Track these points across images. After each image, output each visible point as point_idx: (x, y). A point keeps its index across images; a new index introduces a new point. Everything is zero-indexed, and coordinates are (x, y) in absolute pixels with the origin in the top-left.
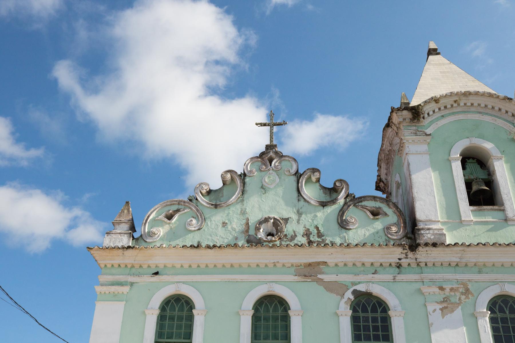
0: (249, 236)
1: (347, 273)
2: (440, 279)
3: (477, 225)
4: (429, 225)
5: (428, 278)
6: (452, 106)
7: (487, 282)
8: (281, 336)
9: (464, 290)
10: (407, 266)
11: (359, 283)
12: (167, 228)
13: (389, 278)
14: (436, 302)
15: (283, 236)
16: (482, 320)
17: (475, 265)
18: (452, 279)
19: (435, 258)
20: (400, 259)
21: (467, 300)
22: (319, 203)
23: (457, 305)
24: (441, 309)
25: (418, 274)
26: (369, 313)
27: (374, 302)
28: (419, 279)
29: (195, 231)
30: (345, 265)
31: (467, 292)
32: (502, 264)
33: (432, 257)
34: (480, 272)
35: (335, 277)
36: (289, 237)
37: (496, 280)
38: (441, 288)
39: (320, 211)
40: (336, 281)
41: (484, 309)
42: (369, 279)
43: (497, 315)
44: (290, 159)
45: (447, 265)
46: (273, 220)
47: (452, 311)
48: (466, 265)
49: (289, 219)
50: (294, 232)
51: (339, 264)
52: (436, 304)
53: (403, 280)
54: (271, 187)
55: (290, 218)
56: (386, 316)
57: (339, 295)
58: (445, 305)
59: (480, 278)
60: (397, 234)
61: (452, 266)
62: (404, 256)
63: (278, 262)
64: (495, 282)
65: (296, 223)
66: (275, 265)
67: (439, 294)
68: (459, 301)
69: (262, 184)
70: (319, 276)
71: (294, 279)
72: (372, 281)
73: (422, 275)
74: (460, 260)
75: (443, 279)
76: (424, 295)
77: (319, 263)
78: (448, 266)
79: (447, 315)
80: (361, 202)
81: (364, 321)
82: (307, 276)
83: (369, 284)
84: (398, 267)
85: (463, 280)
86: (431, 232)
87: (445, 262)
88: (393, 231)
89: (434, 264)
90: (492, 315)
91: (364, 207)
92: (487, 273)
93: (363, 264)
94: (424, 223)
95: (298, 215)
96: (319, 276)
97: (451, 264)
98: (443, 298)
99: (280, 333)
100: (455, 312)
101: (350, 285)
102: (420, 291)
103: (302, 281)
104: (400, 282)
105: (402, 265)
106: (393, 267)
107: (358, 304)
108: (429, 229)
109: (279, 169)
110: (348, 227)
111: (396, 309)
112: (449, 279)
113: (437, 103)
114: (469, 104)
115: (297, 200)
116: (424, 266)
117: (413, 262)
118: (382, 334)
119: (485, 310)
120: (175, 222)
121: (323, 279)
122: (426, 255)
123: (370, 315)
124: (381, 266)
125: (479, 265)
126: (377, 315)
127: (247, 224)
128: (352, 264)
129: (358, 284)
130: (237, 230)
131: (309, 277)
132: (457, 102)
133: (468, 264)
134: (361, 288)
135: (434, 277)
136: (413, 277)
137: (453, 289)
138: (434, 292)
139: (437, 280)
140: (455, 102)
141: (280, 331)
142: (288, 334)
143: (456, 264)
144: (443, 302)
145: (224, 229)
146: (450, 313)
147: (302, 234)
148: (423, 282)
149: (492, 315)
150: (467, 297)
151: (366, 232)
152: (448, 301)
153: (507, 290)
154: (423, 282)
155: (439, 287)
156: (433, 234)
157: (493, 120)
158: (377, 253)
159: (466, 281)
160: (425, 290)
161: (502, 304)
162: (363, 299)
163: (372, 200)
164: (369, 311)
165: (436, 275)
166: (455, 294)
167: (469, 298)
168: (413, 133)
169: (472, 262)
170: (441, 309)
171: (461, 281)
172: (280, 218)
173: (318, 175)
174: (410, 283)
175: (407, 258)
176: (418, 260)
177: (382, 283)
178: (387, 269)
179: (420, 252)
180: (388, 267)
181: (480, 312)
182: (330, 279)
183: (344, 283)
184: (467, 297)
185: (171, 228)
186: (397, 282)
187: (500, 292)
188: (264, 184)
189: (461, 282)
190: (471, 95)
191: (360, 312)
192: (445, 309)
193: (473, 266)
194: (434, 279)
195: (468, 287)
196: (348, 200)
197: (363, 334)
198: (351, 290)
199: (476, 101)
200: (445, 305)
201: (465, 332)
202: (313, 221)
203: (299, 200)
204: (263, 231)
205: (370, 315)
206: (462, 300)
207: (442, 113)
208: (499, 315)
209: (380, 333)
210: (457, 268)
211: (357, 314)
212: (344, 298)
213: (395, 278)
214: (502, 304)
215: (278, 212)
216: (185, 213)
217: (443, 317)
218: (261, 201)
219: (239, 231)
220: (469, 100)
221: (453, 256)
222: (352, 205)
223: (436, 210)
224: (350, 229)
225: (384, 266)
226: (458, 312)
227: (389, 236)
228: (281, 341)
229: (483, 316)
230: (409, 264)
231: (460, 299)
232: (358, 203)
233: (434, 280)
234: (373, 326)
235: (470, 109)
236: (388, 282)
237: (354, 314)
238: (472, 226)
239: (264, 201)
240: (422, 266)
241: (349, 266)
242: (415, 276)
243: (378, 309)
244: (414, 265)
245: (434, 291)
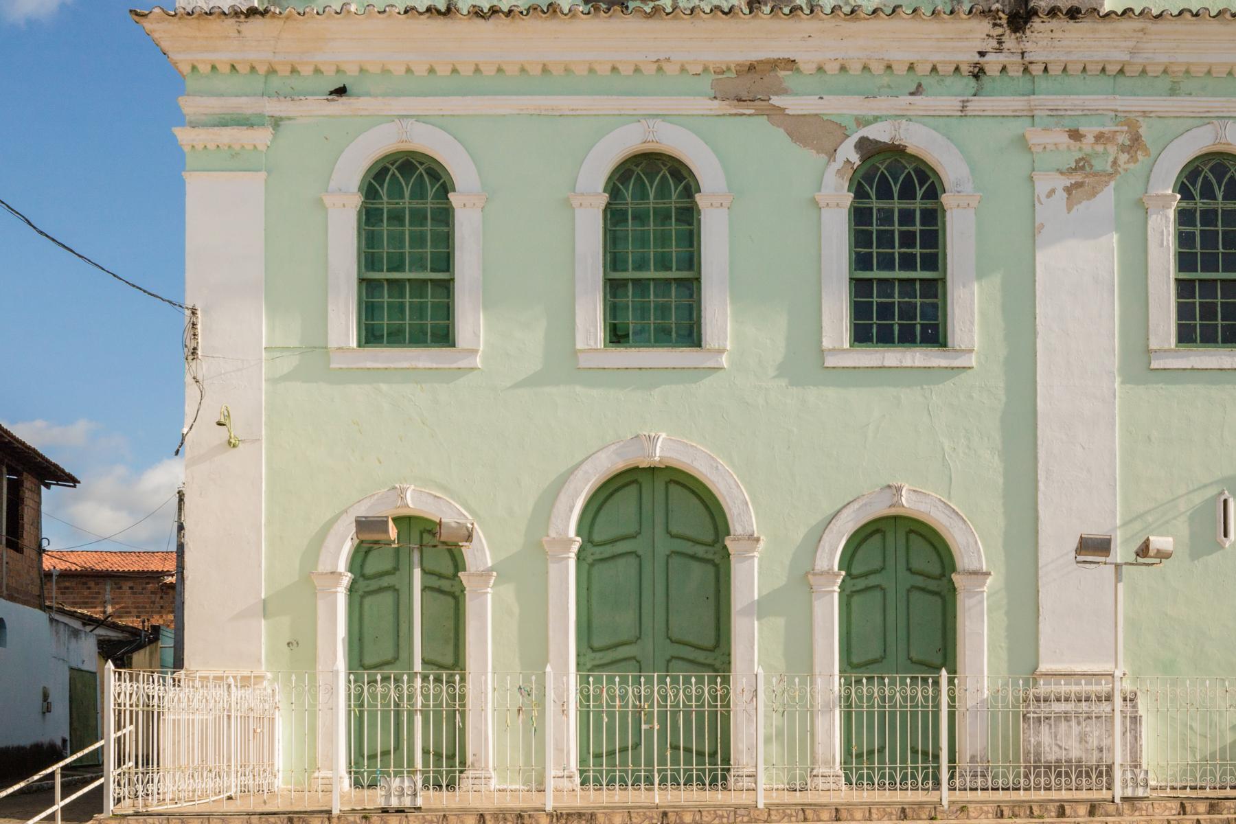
1: (846, 92)
2: (1077, 110)
5: (1046, 108)
7: (1187, 117)
8: (677, 262)
9: (1129, 140)
10: (999, 74)
11: (876, 119)
14: (1058, 170)
16: (1160, 216)
17: (1165, 72)
18: (1103, 110)
19: (1070, 52)
20: (982, 54)
21: (1131, 166)
23: (1106, 179)
24: (1068, 190)
25: (1023, 95)
26: (893, 199)
27: (909, 172)
28: (1023, 110)
30: (843, 68)
31: (1135, 143)
32: (1228, 70)
33: (1062, 47)
34: (1173, 92)
37: (1208, 112)
38: (1075, 135)
40: (817, 115)
41: (1167, 188)
42: (900, 110)
43: (1196, 204)
47: (1094, 194)
48: (1144, 72)
51: (827, 67)
52: (1058, 175)
56: (934, 206)
57: (822, 152)
58: (1078, 178)
61: (1107, 73)
62: (994, 43)
64: (1205, 119)
68: (1112, 167)
70: (776, 101)
71: (711, 110)
72: (908, 113)
73: (1032, 97)
74: (1131, 57)
75: (1083, 110)
76: (1032, 153)
77: (774, 64)
78: (1098, 73)
79: (1080, 203)
81: (881, 221)
82: (744, 99)
83: (899, 123)
84: (976, 76)
85: (1130, 112)
87: (1092, 62)
89: (1065, 69)
90: (1184, 204)
92: (1190, 94)
93: (889, 67)
96: (776, 101)
97: (1108, 67)
98: (1077, 162)
99: (674, 254)
100: (1099, 196)
101: (852, 124)
102: (1022, 142)
103: (731, 115)
104: (978, 119)
105: (987, 68)
106: (965, 76)
107: (868, 178)
111: (959, 189)
112: (1097, 110)
116: (1041, 73)
117: (1013, 63)
118: (921, 254)
119: (1170, 191)
122: (1049, 43)
123: (897, 205)
124: (933, 74)
125: (1174, 72)
126: (914, 204)
128: (860, 67)
131: (749, 103)
133: (1148, 69)
134: (880, 133)
137: (1103, 137)
138: (1056, 144)
139: (1069, 113)
141: (676, 247)
142: (696, 254)
143: (1119, 68)
144: (1075, 169)
146: (1088, 200)
148: (1033, 116)
149: (1184, 204)
150: (1133, 159)
152: (1087, 169)
153: (1230, 140)
154: (1033, 116)
155: (1070, 131)
159: (1137, 114)
160: (1036, 138)
161: (1211, 176)
162: (882, 164)
164: (896, 195)
165: (1068, 97)
166: (1105, 149)
167: (1137, 160)
169: (1159, 64)
170: (1068, 190)
171: (1125, 114)
174: (1000, 119)
176: (1028, 58)
178: (948, 81)
180: (950, 76)
181: (1157, 196)
184: (1132, 157)
187: (1212, 143)
191: (874, 197)
192: (1077, 188)
193: (1159, 74)
194: (1060, 110)
195: (1140, 130)
197: (877, 253)
198: (854, 139)
200: (1078, 178)
201: (1115, 245)
205: (897, 205)
206: (1119, 166)
208: (1200, 204)
209: (918, 250)
210: (1121, 80)
211: (865, 203)
212: (835, 161)
214: (1211, 176)
217: (1069, 210)
221: (1115, 47)
225: (941, 73)
226: (1107, 197)
228: (677, 272)
229: (1163, 207)
230: (1004, 69)
231: (1115, 163)
233: (1060, 113)
234: (901, 233)
236: (948, 116)
237: (859, 203)
240: (1034, 73)
241: (851, 72)
242: (1017, 101)
243: (918, 188)
244: (1015, 71)
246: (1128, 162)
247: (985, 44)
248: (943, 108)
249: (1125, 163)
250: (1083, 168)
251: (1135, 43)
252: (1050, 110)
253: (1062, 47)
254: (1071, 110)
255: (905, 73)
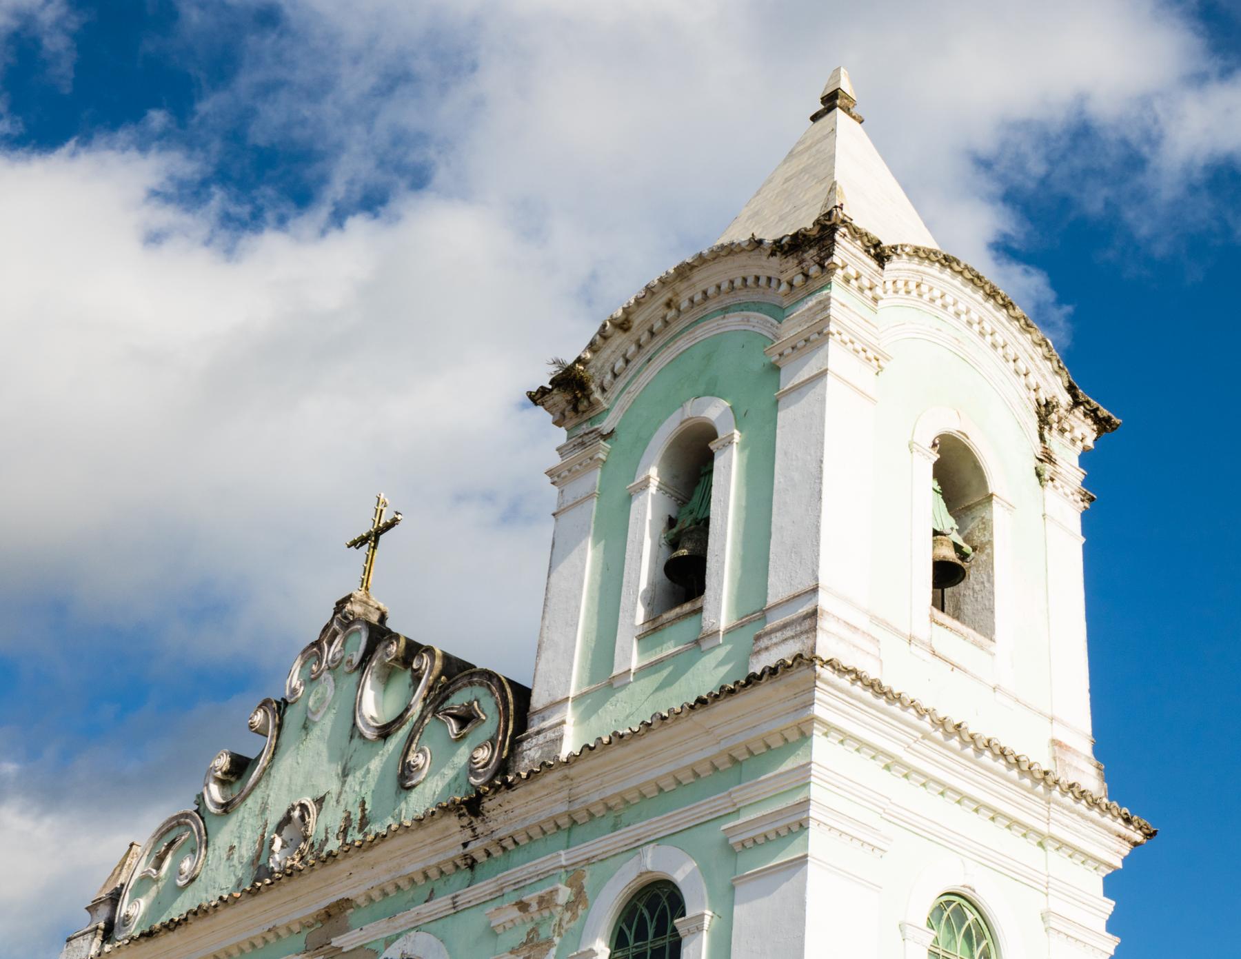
0: (260, 866)
3: (644, 677)
4: (549, 717)
5: (508, 884)
6: (666, 323)
7: (622, 852)
11: (398, 936)
12: (153, 891)
13: (446, 906)
15: (308, 848)
18: (554, 869)
20: (465, 845)
22: (380, 730)
29: (186, 885)
34: (615, 827)
35: (359, 934)
36: (317, 846)
37: (639, 840)
38: (523, 906)
39: (377, 754)
40: (362, 946)
44: (359, 627)
45: (552, 829)
46: (300, 810)
48: (592, 815)
49: (327, 797)
50: (327, 829)
53: (470, 902)
54: (317, 720)
55: (328, 792)
59: (606, 846)
60: (485, 769)
62: (469, 832)
63: (274, 926)
65: (335, 803)
66: (278, 936)
67: (524, 923)
69: (305, 715)
75: (538, 875)
80: (447, 698)
86: (541, 738)
87: (544, 822)
88: (478, 763)
91: (448, 711)
92: (629, 825)
94: (541, 715)
95: (342, 779)
98: (528, 934)
104: (467, 911)
108: (538, 733)
109: (338, 662)
110: (409, 784)
112: (548, 871)
113: (626, 330)
114: (698, 298)
115: (349, 738)
120: (166, 875)
121: (342, 948)
127: (263, 836)
129: (395, 941)
130: (245, 860)
132: (672, 304)
135: (518, 874)
136: (484, 888)
138: (512, 921)
140: (669, 305)
145: (227, 864)
147: (336, 832)
151: (439, 783)
155: (517, 904)
156: (540, 746)
157: (743, 320)
158: (422, 844)
159: (582, 864)
163: (465, 685)
165: (524, 866)
168: (578, 444)
171: (574, 868)
172: (313, 800)
173: (394, 651)
175: (476, 837)
176: (497, 836)
177: (434, 923)
178: (452, 879)
179: (492, 813)
182: (352, 944)
183: (373, 947)
184: (574, 914)
185: (158, 893)
186: (462, 910)
188: (310, 715)
189: (574, 870)
190: (694, 271)
194: (521, 881)
196: (428, 701)
199: (705, 280)
202: (361, 788)
203: (352, 737)
204: (282, 847)
207: (648, 351)
213: (456, 902)
215: (313, 785)
216: (183, 843)
218: (295, 764)
219: (246, 863)
220: (694, 285)
222: (430, 715)
223: (571, 666)
224: (413, 787)
227: (472, 780)
232: (442, 703)
235: (705, 309)
236: (446, 916)
238: (630, 686)
239: (300, 761)
244: (496, 852)
245: (511, 919)
246: (570, 921)
247: (463, 835)
248: (440, 910)
249: (568, 922)
250: (531, 940)
251: (567, 792)
252: (515, 884)
253: (516, 817)
254: (530, 878)
255: (423, 882)
